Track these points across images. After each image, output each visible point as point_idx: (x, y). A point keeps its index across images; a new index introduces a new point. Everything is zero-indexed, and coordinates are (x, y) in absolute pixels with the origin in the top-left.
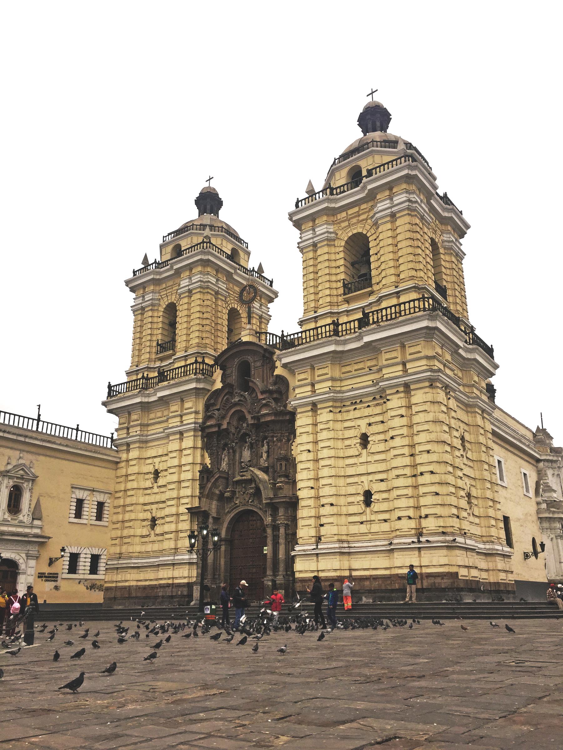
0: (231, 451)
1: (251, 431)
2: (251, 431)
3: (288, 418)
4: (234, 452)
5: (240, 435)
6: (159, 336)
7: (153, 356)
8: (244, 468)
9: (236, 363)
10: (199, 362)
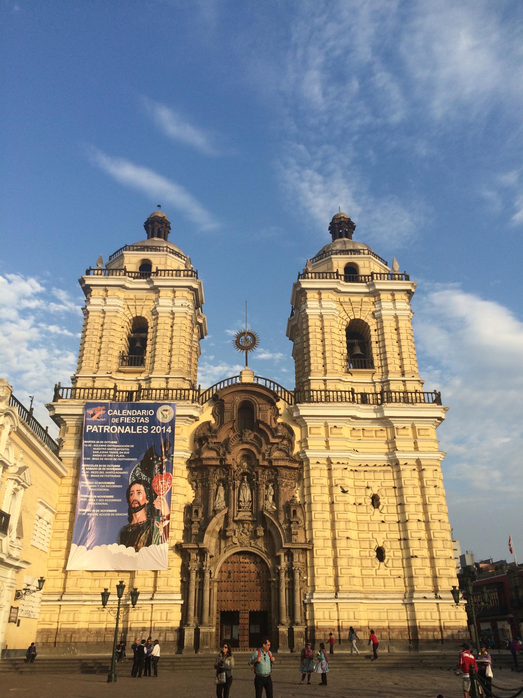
0: (231, 488)
2: (257, 473)
4: (234, 489)
5: (240, 473)
7: (115, 367)
8: (240, 507)
9: (237, 401)
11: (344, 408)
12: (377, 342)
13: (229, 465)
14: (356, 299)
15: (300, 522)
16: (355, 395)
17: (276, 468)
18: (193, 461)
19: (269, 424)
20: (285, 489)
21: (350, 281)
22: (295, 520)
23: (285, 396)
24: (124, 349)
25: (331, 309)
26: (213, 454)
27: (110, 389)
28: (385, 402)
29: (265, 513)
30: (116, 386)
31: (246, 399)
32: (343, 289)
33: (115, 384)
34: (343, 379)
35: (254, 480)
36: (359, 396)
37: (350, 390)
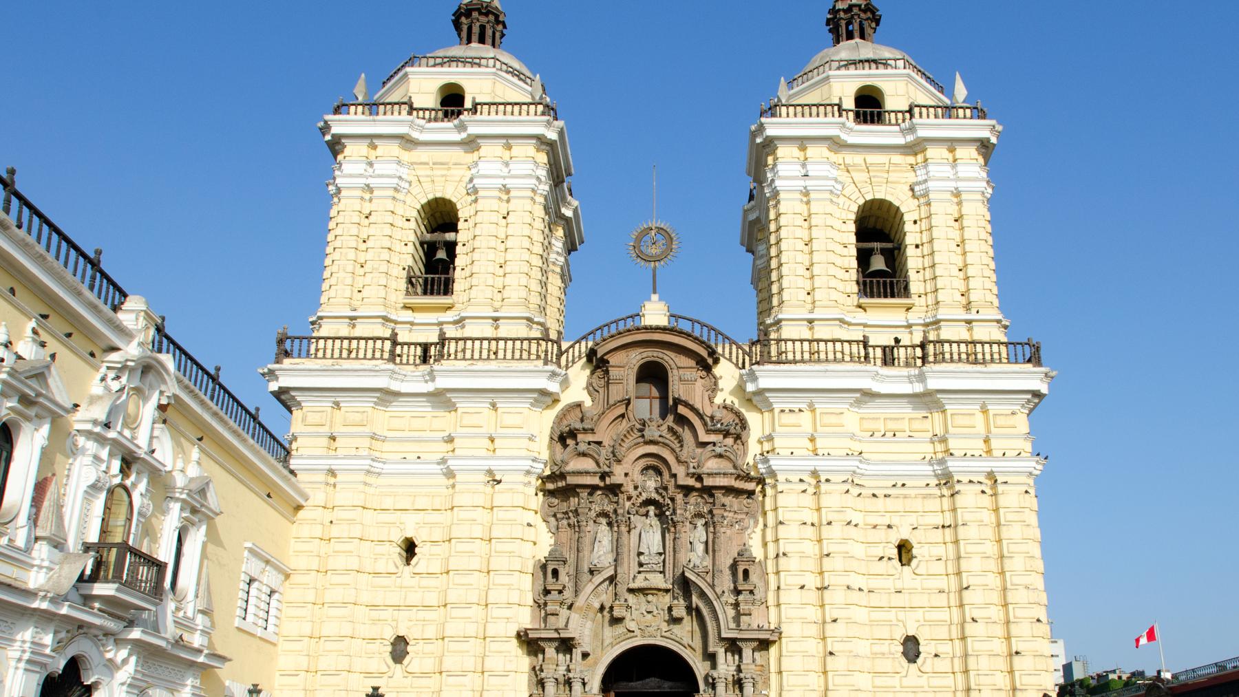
1: (672, 499)
2: (672, 499)
3: (750, 486)
5: (640, 500)
6: (407, 256)
8: (641, 565)
9: (634, 362)
10: (551, 341)
11: (847, 374)
12: (917, 246)
13: (620, 486)
14: (874, 158)
15: (756, 592)
16: (871, 350)
17: (709, 491)
18: (548, 477)
19: (698, 406)
20: (728, 532)
21: (865, 122)
22: (746, 587)
23: (731, 353)
24: (410, 262)
25: (826, 178)
26: (588, 464)
27: (383, 339)
28: (930, 363)
29: (687, 574)
30: (394, 335)
31: (652, 359)
32: (851, 139)
33: (393, 330)
34: (847, 319)
35: (667, 513)
36: (879, 352)
37: (862, 339)
